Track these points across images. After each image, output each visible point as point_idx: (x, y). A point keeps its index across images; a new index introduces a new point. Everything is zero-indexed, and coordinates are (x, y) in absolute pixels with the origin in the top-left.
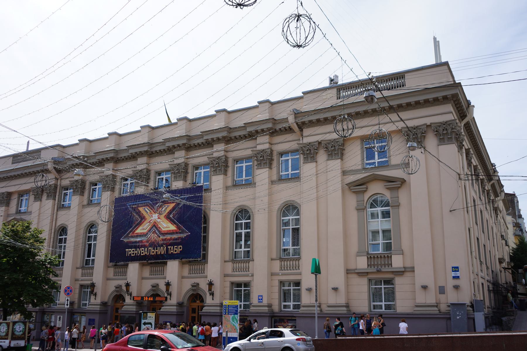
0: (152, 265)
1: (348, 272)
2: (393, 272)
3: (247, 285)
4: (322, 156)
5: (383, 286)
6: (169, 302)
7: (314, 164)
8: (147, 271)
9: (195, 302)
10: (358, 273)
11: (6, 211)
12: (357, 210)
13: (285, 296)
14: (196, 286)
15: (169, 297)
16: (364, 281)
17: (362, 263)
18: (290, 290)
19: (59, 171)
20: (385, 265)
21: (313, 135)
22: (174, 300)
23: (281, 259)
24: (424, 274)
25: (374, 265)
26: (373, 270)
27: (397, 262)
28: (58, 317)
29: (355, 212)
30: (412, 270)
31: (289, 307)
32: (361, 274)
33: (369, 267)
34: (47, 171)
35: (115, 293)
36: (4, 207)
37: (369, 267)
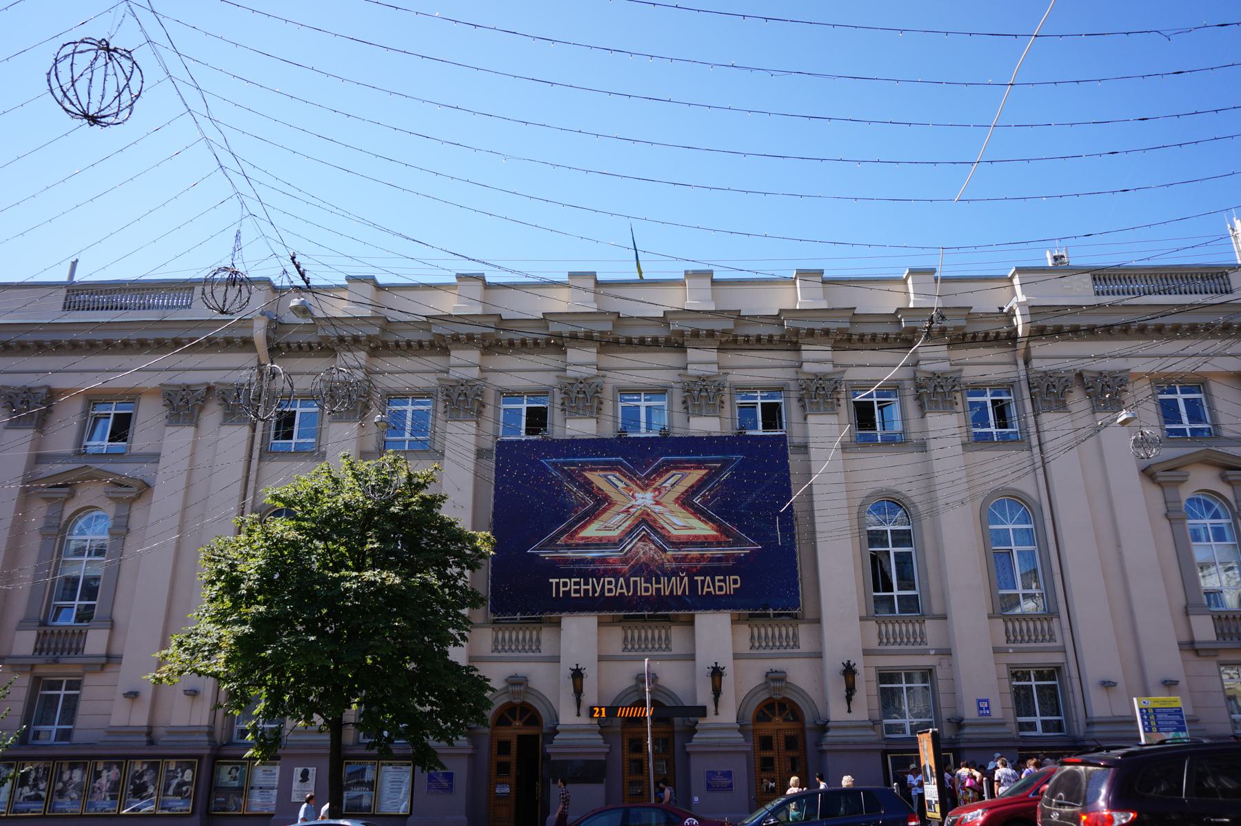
0: (627, 624)
3: (1054, 672)
4: (1078, 401)
6: (711, 719)
8: (615, 638)
9: (769, 720)
11: (37, 444)
13: (1022, 700)
14: (775, 678)
15: (711, 708)
18: (1041, 689)
19: (275, 350)
21: (1054, 356)
22: (728, 714)
23: (1007, 619)
26: (1228, 644)
28: (298, 771)
31: (1032, 726)
34: (247, 344)
35: (763, 696)
36: (31, 431)
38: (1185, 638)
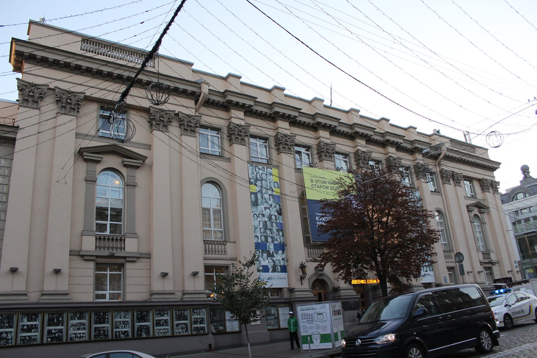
1: (72, 253)
2: (125, 258)
5: (108, 273)
7: (37, 112)
10: (82, 256)
12: (86, 181)
16: (92, 265)
17: (89, 244)
20: (117, 248)
24: (162, 262)
25: (108, 248)
27: (131, 246)
29: (84, 184)
30: (148, 256)
32: (84, 257)
33: (98, 249)
37: (98, 249)
38: (76, 248)
